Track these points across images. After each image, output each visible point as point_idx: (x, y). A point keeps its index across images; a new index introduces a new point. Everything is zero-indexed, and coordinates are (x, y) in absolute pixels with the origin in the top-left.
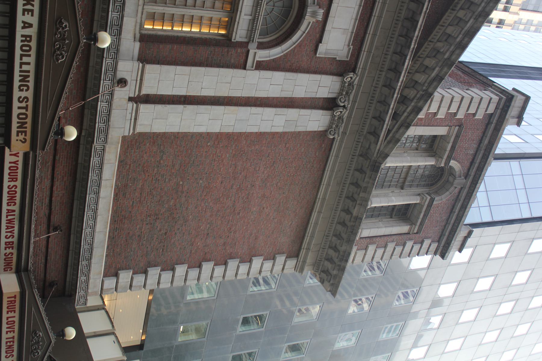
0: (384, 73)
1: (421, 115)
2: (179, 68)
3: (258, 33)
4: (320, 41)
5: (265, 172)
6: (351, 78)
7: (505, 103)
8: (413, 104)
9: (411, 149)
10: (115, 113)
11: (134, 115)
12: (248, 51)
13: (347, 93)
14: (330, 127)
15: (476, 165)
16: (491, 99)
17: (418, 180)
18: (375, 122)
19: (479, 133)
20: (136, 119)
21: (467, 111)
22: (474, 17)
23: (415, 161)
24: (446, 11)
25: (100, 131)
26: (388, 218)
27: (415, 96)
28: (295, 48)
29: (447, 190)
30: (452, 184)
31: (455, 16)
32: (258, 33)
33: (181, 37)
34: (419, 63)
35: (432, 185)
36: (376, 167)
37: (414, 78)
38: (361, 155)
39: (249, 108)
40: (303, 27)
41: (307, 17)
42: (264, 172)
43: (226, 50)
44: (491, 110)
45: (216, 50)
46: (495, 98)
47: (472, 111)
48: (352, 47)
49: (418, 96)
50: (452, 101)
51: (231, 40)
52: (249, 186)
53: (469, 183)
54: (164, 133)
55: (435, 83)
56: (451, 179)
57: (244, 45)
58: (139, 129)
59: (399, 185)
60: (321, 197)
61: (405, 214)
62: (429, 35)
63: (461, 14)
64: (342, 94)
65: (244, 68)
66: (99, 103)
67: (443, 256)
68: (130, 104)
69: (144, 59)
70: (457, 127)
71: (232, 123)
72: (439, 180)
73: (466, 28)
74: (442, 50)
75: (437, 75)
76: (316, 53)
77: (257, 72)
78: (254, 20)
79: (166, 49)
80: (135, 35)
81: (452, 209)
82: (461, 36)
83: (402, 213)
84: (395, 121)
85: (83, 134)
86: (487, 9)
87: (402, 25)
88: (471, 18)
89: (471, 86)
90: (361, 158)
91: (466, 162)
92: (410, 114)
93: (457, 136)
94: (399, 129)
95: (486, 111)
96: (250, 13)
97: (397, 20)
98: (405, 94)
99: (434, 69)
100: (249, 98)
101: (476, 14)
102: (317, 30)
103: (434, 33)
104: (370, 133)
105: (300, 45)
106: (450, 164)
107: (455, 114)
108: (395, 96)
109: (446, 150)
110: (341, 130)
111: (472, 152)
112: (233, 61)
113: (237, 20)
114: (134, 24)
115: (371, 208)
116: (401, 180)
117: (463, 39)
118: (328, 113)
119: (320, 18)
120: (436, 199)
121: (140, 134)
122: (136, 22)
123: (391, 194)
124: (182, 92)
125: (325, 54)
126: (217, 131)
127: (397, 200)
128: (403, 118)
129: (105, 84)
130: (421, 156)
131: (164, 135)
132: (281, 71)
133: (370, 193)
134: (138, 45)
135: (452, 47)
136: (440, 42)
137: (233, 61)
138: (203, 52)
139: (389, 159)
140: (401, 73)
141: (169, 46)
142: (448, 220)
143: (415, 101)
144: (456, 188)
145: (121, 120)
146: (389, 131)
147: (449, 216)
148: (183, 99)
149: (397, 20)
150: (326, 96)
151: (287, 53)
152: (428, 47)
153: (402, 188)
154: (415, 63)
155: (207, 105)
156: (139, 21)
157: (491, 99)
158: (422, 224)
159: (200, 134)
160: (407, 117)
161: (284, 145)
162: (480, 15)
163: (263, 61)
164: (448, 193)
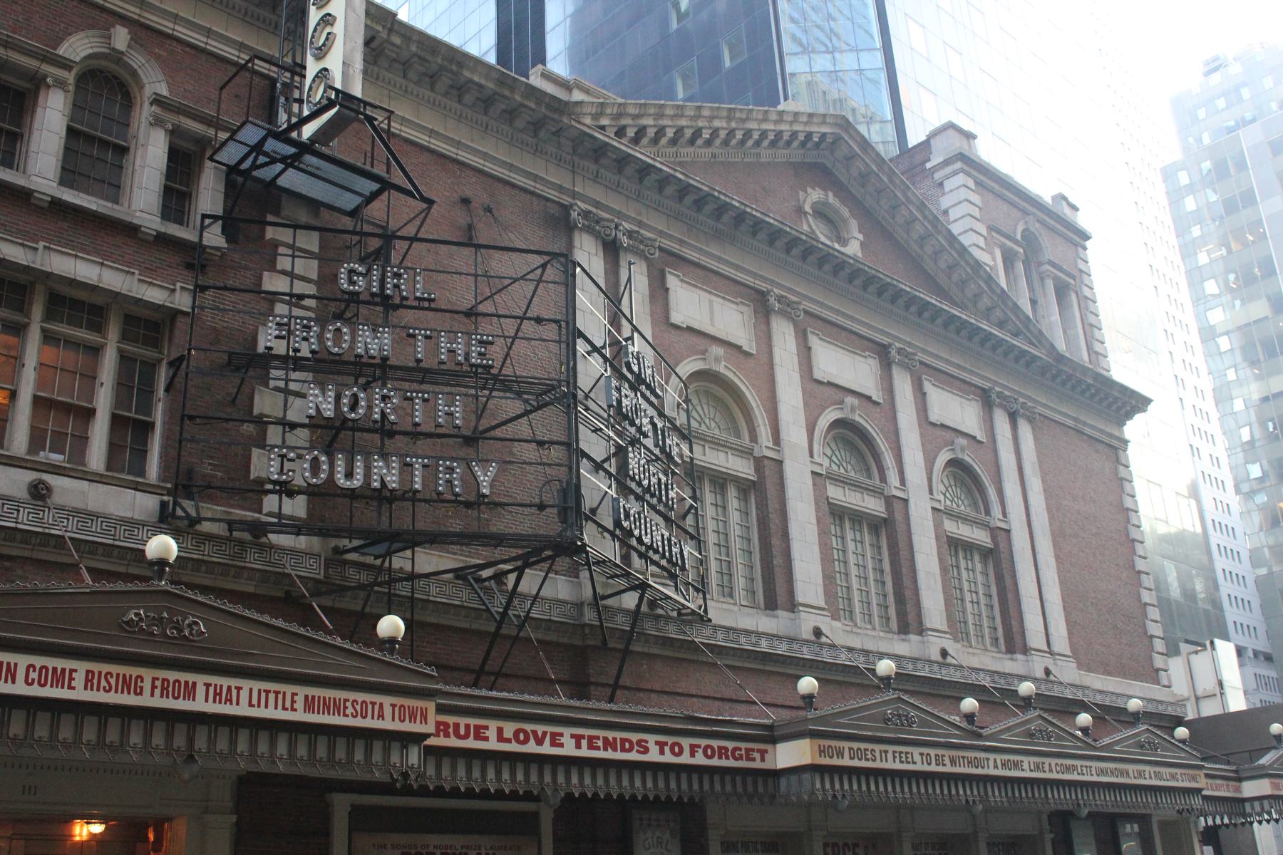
53: (1034, 210)
63: (929, 250)
67: (1087, 238)
75: (986, 283)
86: (931, 217)
92: (1018, 317)
94: (1029, 330)
117: (955, 249)
146: (1031, 343)
158: (1069, 275)
162: (935, 227)
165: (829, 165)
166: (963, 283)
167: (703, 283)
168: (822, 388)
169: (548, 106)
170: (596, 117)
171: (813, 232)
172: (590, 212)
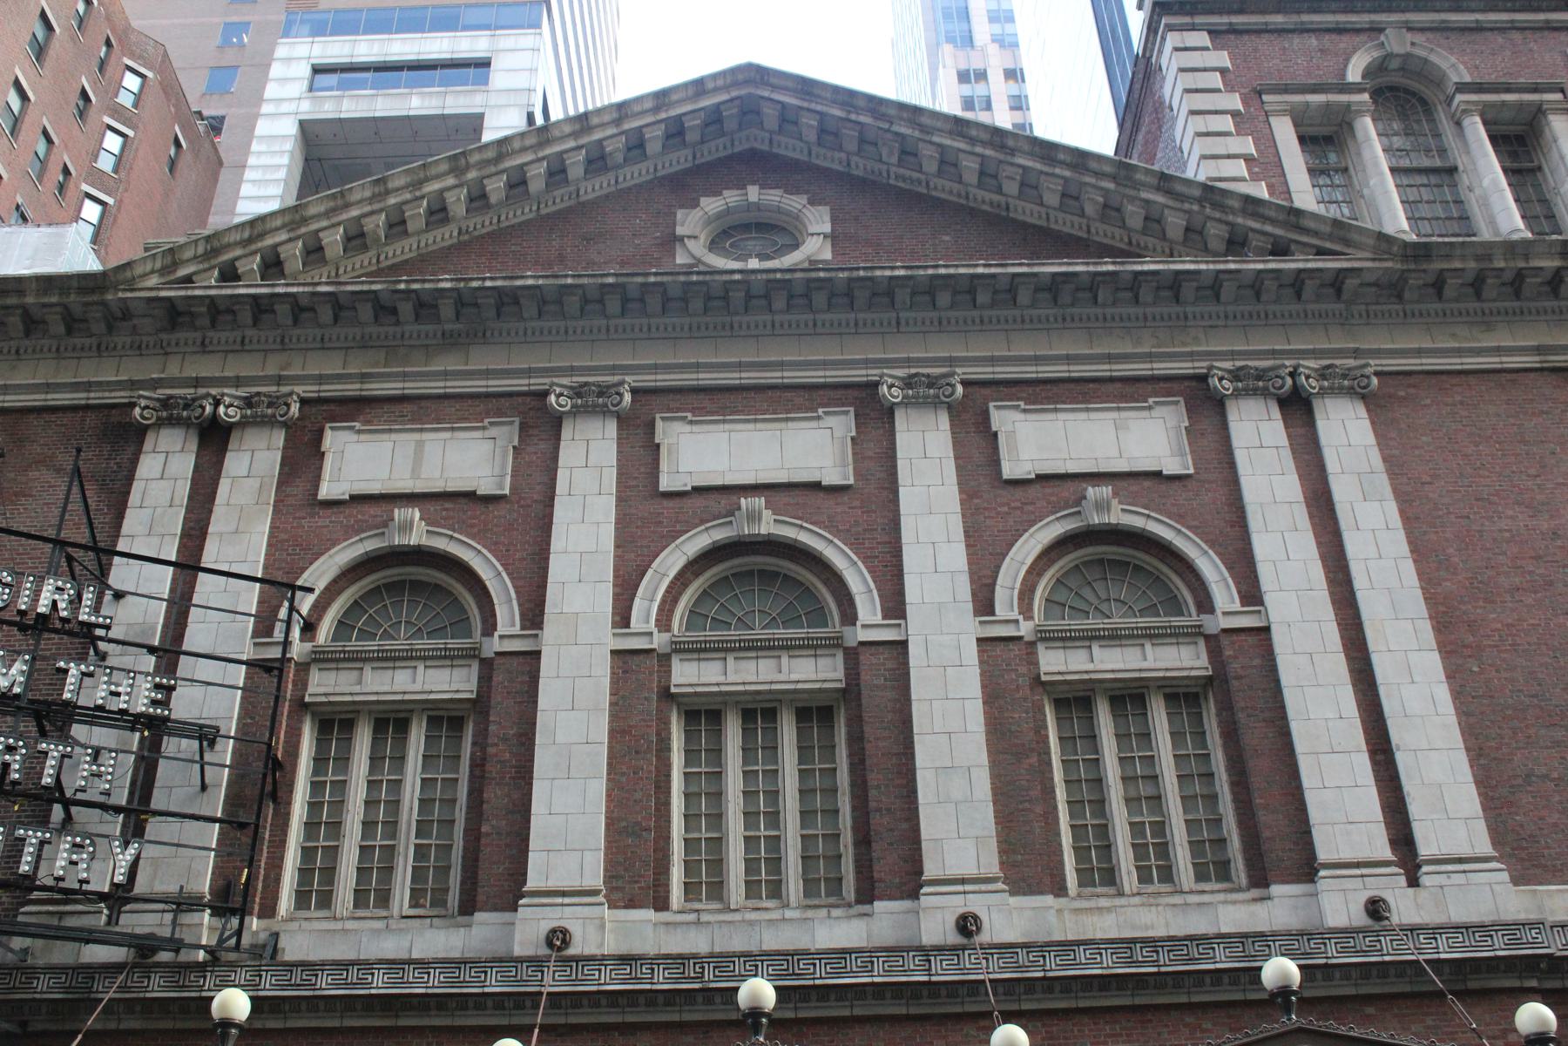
0: (1189, 309)
1: (1261, 191)
2: (1307, 781)
3: (1177, 621)
4: (1157, 475)
5: (1510, 513)
6: (1221, 379)
7: (1175, 14)
8: (1240, 220)
9: (1348, 185)
10: (1458, 915)
11: (1450, 867)
12: (1225, 631)
13: (1259, 378)
14: (1351, 392)
15: (1341, 18)
16: (1176, 49)
17: (1421, 140)
18: (1308, 292)
19: (1263, 43)
20: (1460, 861)
21: (1219, 91)
22: (1009, 158)
23: (1377, 164)
24: (1014, 221)
25: (1515, 942)
26: (1545, 180)
27: (1220, 221)
28: (1188, 528)
29: (1426, 61)
30: (1408, 56)
31: (1019, 198)
32: (1177, 621)
33: (1233, 793)
34: (1143, 240)
35: (1424, 102)
36: (1418, 252)
37: (1181, 239)
38: (1400, 297)
39: (1359, 595)
40: (1138, 522)
41: (1113, 521)
42: (1511, 517)
43: (1235, 683)
44: (1202, 39)
45: (1242, 704)
46: (1172, 39)
47: (1216, 80)
48: (1151, 400)
49: (1218, 215)
50: (1208, 134)
51: (1210, 678)
52: (1559, 543)
53: (1394, 17)
54: (1478, 783)
55: (1179, 188)
56: (1394, 64)
57: (1214, 643)
58: (1484, 846)
59: (1446, 179)
60: (1537, 358)
61: (1521, 140)
62: (1080, 238)
64: (1266, 389)
65: (1267, 629)
66: (1443, 956)
68: (1425, 880)
69: (1307, 868)
70: (1265, 98)
71: (1408, 625)
72: (1407, 91)
73: (1038, 166)
74: (1101, 199)
75: (1158, 189)
76: (1188, 476)
77: (1267, 598)
78: (1150, 637)
79: (1271, 821)
80: (1255, 900)
81: (1471, 29)
82: (1057, 171)
83: (1520, 143)
84: (1293, 247)
85: (1534, 983)
86: (985, 136)
87: (1073, 305)
88: (1012, 164)
89: (1162, 103)
90: (1407, 295)
91: (1342, 45)
93: (1286, 89)
95: (1207, 49)
96: (1137, 650)
97: (1064, 319)
98: (1222, 247)
99: (1147, 202)
100: (1333, 603)
101: (1001, 157)
102: (1134, 488)
103: (1066, 229)
104: (1339, 292)
105: (1180, 518)
106: (1358, 79)
107: (1235, 114)
108: (1232, 266)
109: (1328, 104)
110: (1351, 362)
111: (1313, 41)
112: (1257, 662)
113: (1161, 674)
114: (1231, 908)
115: (1529, 227)
116: (1434, 179)
117: (1062, 163)
118: (1318, 405)
119: (1106, 491)
120: (1456, 79)
121: (1496, 843)
122: (1225, 902)
123: (1477, 192)
124: (1363, 762)
125: (1182, 455)
126: (1436, 656)
127: (1486, 170)
128: (1279, 232)
129: (1389, 951)
130: (1359, 154)
131: (1485, 782)
132: (1250, 544)
133: (1491, 245)
134: (1276, 889)
135: (1088, 179)
136: (1083, 210)
137: (1257, 662)
138: (1254, 735)
139: (1389, 229)
140: (1178, 273)
141: (1263, 817)
142: (1502, 30)
143: (1230, 218)
144: (1413, 44)
145: (1472, 895)
146: (1321, 252)
147: (1491, 29)
148: (1380, 757)
149: (1064, 319)
150: (1279, 425)
151: (1206, 542)
152: (1103, 233)
153: (1452, 170)
154: (1146, 247)
155: (1378, 695)
156: (1221, 897)
157: (1176, 49)
158: (1536, 89)
159: (1457, 695)
160: (1273, 221)
161: (1427, 488)
162: (1002, 147)
163: (1239, 592)
164: (1433, 58)
165: (765, 147)
166: (1110, 210)
167: (413, 421)
168: (687, 503)
169: (82, 290)
170: (163, 271)
171: (699, 261)
172: (171, 397)
